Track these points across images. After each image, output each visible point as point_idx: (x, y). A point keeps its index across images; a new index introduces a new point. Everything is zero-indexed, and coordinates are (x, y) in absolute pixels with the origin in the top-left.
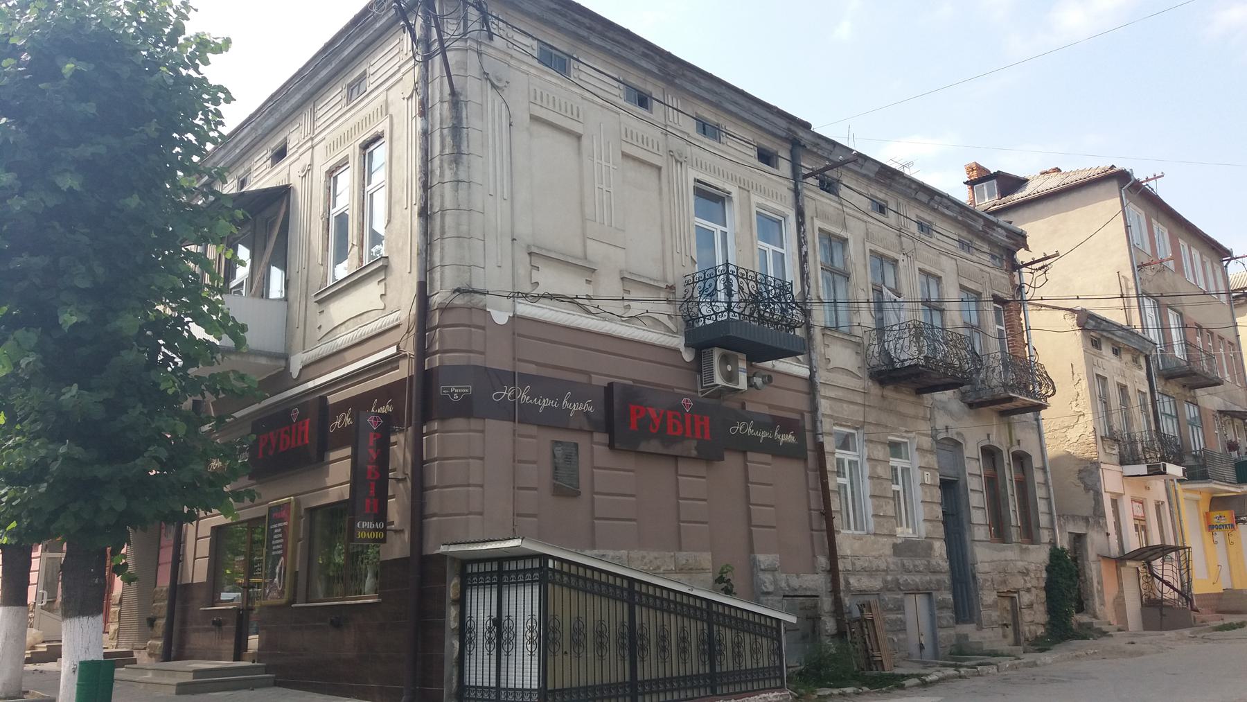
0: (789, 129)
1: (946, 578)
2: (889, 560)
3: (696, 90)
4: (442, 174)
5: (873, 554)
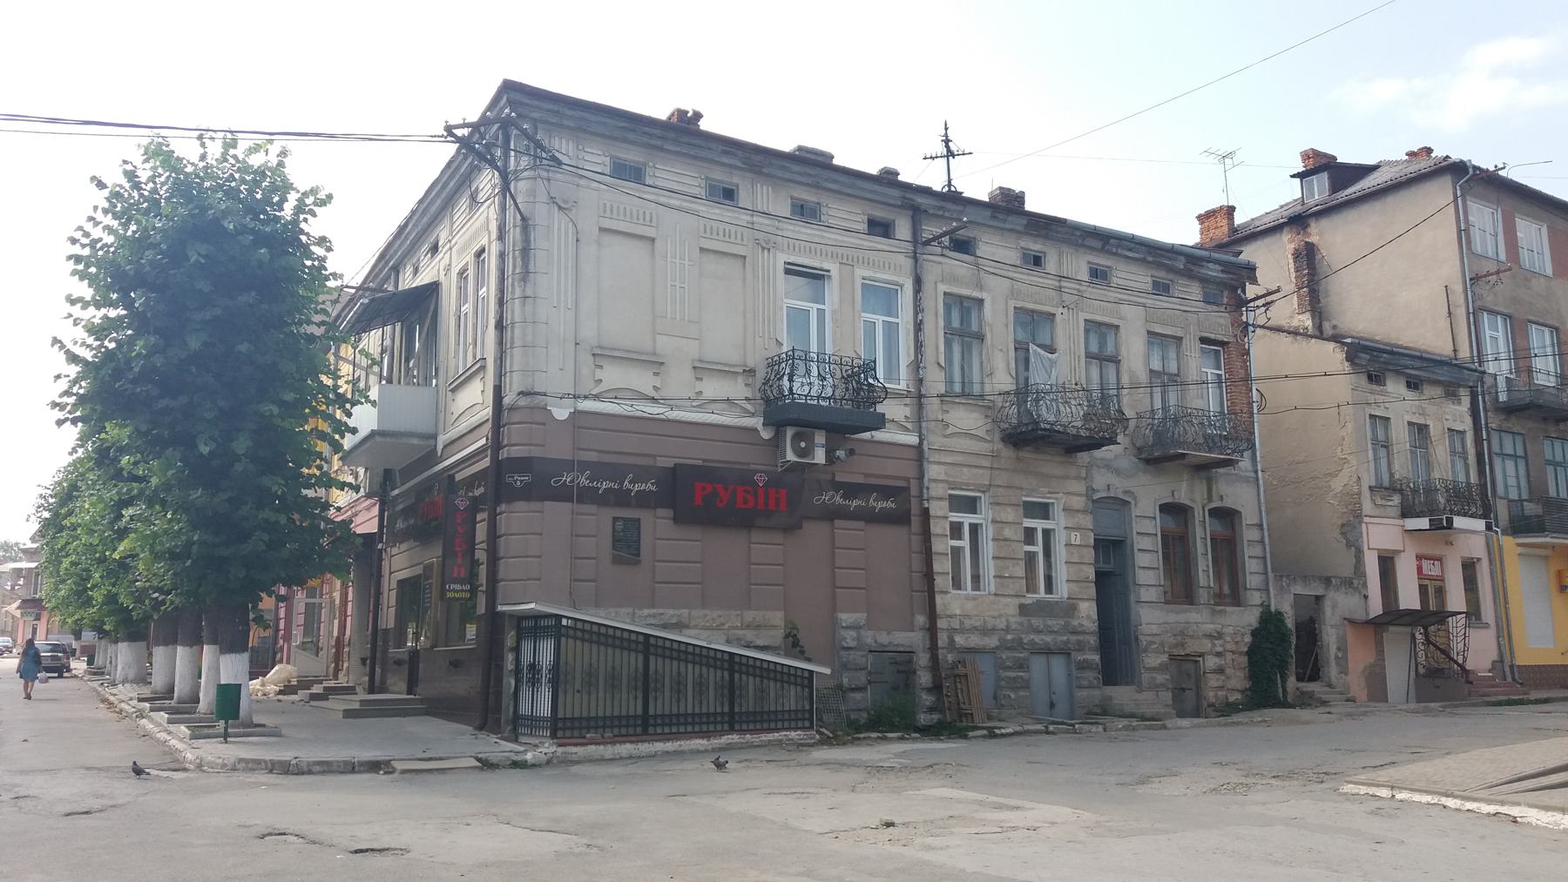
0: (905, 198)
1: (1093, 640)
2: (1012, 620)
3: (788, 175)
4: (513, 293)
5: (992, 613)
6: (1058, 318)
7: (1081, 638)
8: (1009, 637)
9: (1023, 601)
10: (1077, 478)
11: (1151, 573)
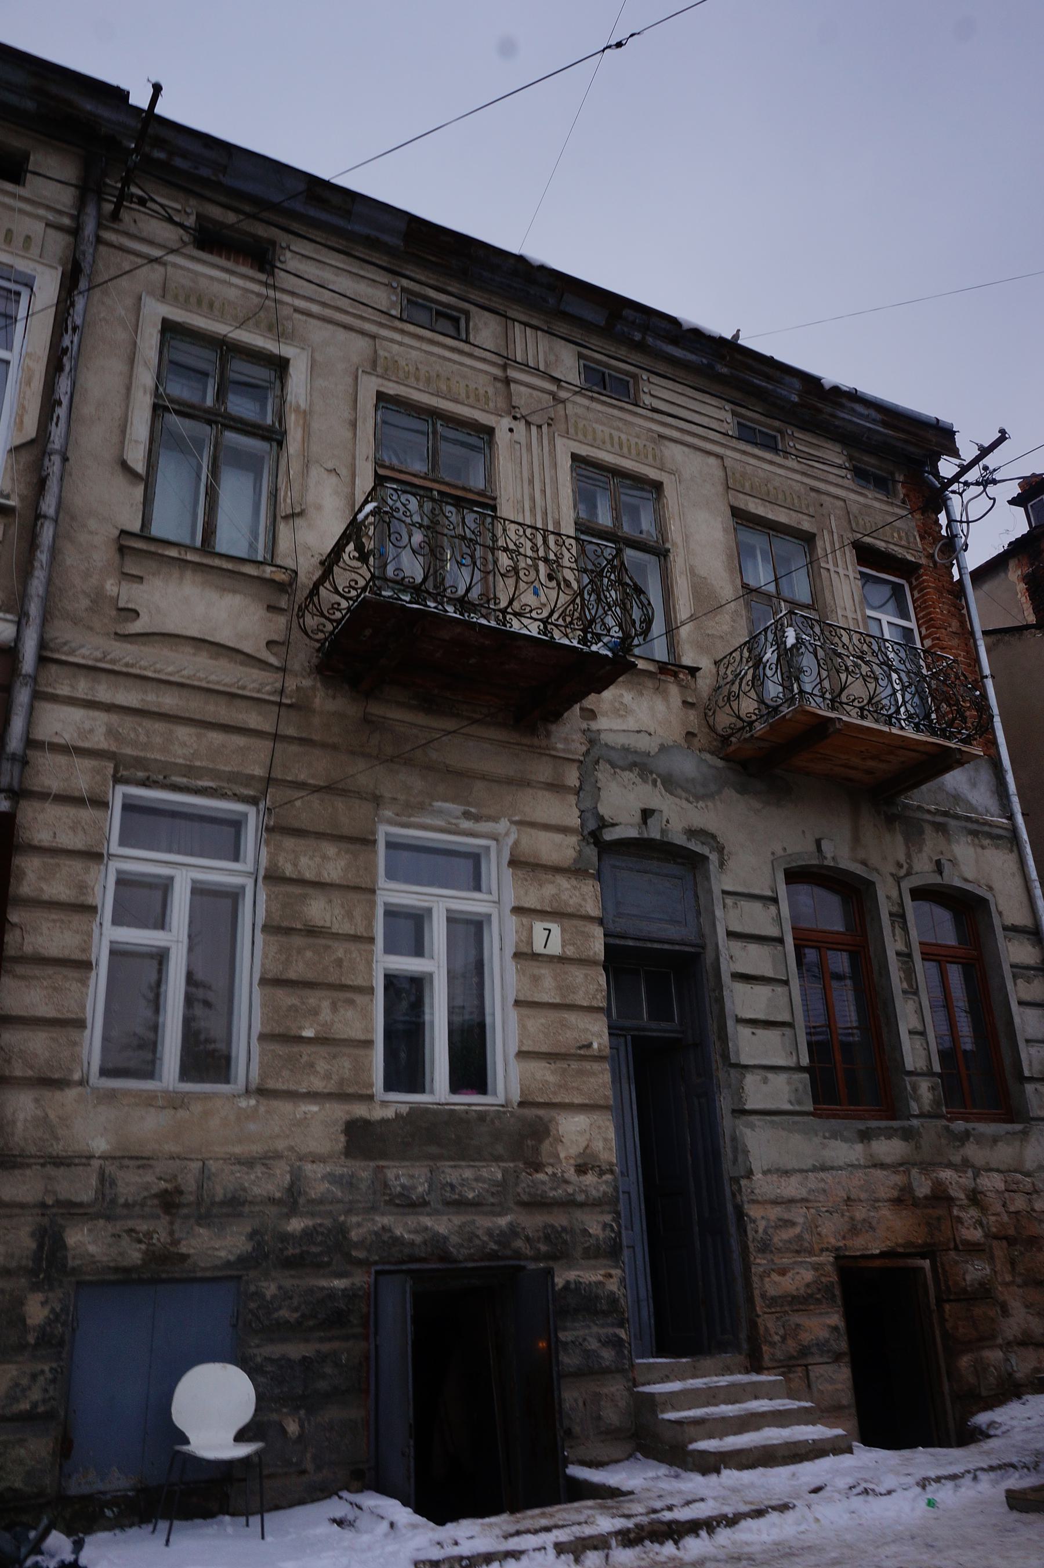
5: (237, 1150)
6: (502, 437)
7: (559, 1219)
8: (296, 1225)
9: (360, 1110)
10: (556, 787)
11: (772, 1036)
